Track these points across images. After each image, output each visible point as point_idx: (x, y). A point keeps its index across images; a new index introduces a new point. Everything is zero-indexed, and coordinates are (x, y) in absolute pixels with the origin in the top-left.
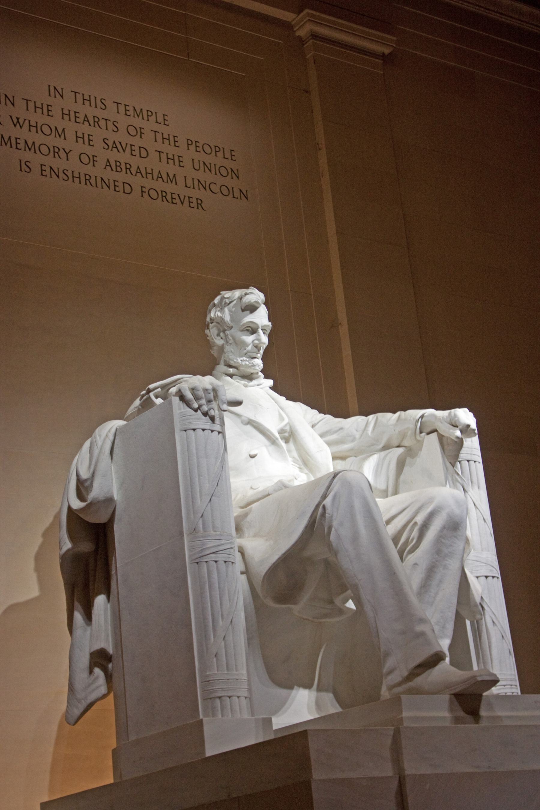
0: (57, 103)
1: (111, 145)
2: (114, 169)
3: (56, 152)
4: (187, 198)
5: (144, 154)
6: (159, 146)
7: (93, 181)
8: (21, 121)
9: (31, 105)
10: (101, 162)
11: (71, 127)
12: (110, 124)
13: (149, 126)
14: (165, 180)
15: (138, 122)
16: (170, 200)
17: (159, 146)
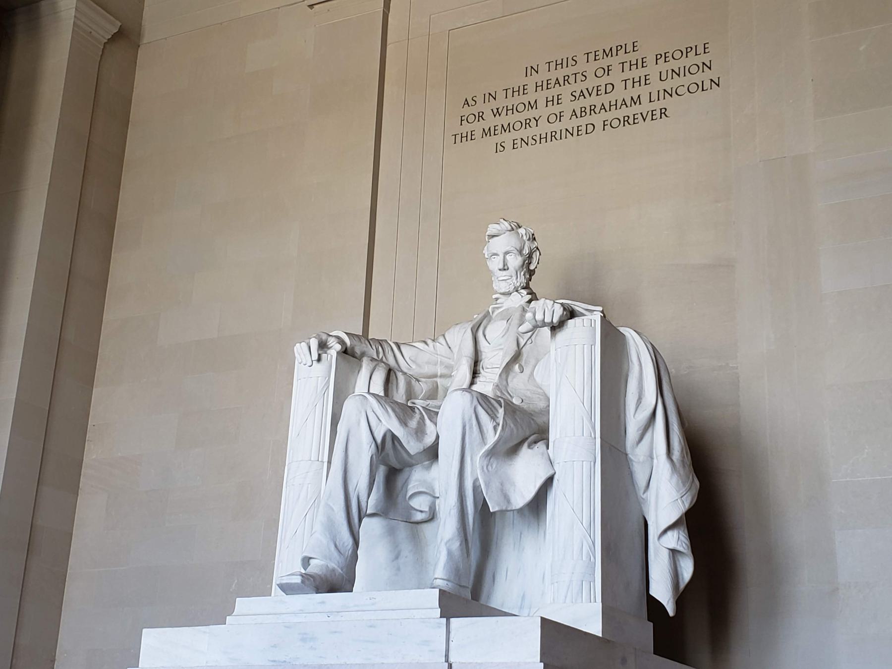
0: (531, 81)
1: (577, 95)
2: (579, 115)
3: (527, 123)
4: (650, 113)
5: (609, 88)
6: (628, 74)
7: (558, 136)
8: (500, 111)
9: (510, 92)
10: (567, 114)
11: (541, 96)
12: (579, 77)
13: (615, 61)
14: (629, 105)
15: (605, 62)
16: (632, 122)
17: (628, 74)
